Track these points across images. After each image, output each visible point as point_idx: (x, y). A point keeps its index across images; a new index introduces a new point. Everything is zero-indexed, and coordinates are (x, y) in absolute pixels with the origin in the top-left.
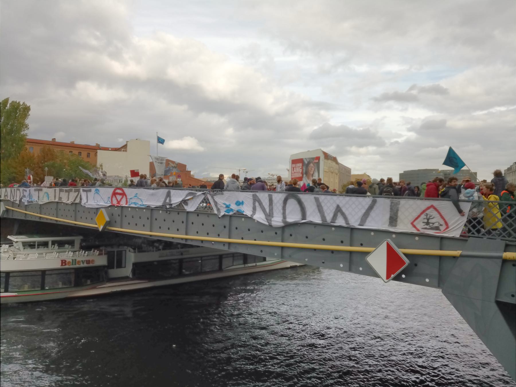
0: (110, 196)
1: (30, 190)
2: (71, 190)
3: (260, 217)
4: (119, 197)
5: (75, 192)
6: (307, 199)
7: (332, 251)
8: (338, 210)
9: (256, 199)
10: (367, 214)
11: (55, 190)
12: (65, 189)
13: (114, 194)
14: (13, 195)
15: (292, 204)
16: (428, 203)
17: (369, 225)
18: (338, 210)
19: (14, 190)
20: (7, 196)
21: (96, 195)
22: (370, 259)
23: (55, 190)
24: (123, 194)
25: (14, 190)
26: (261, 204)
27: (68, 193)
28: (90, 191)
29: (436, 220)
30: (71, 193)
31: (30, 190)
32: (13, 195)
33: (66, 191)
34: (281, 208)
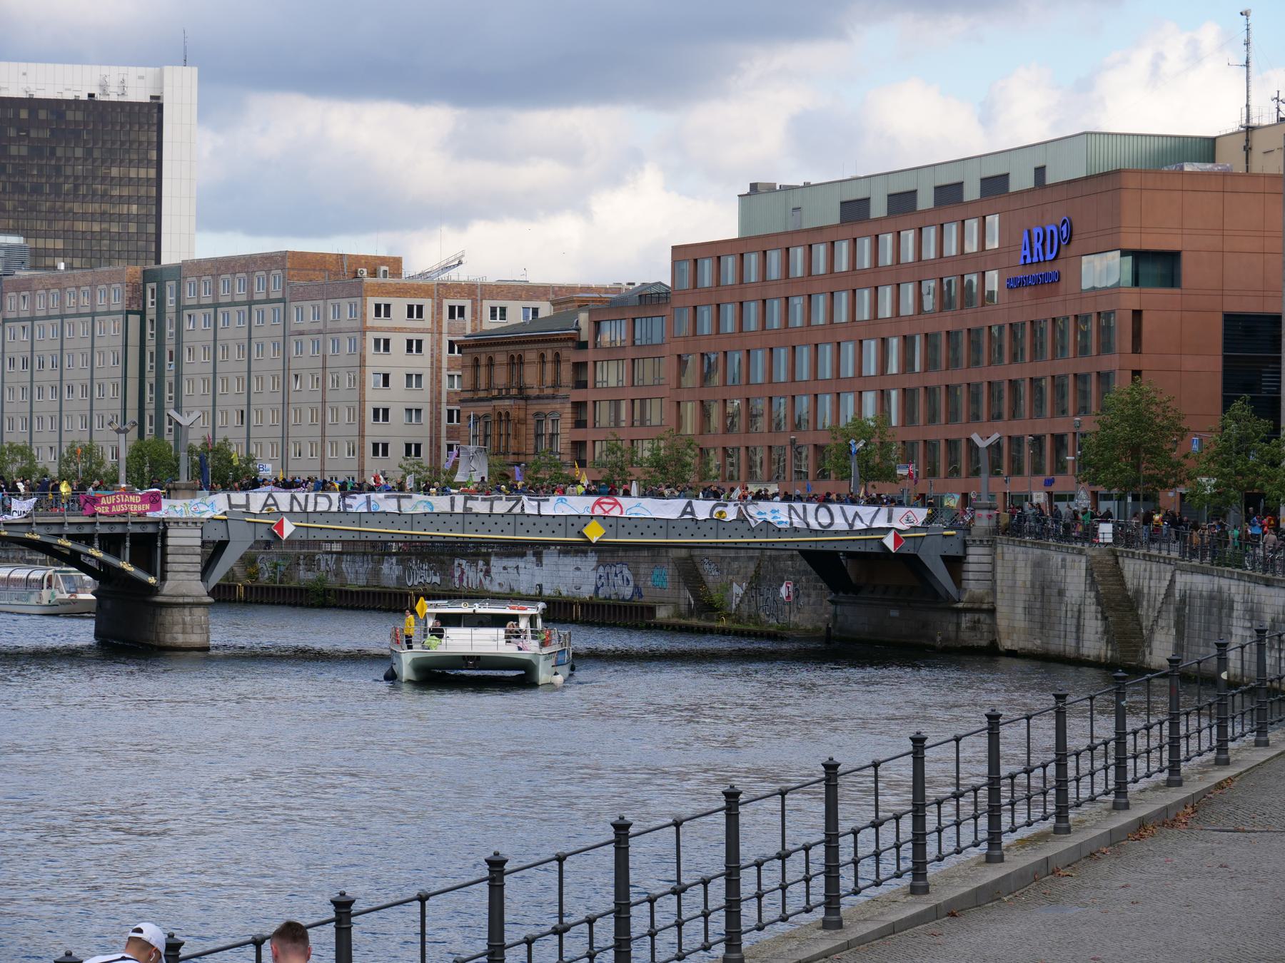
0: (591, 506)
1: (368, 498)
2: (501, 499)
3: (797, 522)
4: (606, 507)
5: (507, 500)
6: (835, 508)
7: (854, 540)
8: (857, 514)
9: (791, 508)
10: (874, 517)
11: (452, 500)
12: (480, 497)
13: (598, 503)
14: (303, 504)
15: (823, 511)
16: (908, 509)
17: (875, 525)
18: (857, 514)
19: (307, 496)
20: (276, 504)
21: (560, 504)
22: (885, 541)
23: (452, 500)
24: (616, 503)
25: (307, 496)
26: (796, 512)
27: (488, 503)
28: (548, 500)
29: (912, 518)
30: (496, 503)
31: (368, 498)
32: (303, 504)
33: (484, 500)
34: (813, 514)
